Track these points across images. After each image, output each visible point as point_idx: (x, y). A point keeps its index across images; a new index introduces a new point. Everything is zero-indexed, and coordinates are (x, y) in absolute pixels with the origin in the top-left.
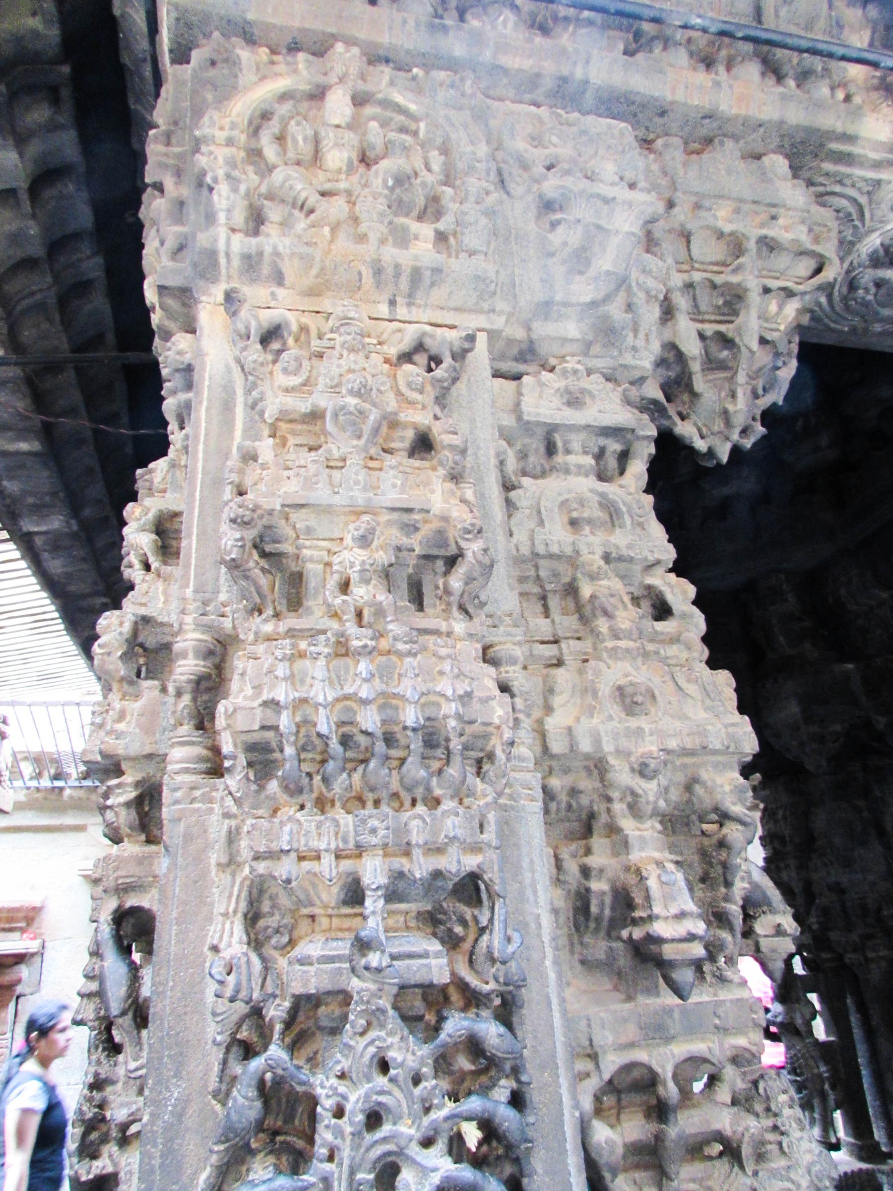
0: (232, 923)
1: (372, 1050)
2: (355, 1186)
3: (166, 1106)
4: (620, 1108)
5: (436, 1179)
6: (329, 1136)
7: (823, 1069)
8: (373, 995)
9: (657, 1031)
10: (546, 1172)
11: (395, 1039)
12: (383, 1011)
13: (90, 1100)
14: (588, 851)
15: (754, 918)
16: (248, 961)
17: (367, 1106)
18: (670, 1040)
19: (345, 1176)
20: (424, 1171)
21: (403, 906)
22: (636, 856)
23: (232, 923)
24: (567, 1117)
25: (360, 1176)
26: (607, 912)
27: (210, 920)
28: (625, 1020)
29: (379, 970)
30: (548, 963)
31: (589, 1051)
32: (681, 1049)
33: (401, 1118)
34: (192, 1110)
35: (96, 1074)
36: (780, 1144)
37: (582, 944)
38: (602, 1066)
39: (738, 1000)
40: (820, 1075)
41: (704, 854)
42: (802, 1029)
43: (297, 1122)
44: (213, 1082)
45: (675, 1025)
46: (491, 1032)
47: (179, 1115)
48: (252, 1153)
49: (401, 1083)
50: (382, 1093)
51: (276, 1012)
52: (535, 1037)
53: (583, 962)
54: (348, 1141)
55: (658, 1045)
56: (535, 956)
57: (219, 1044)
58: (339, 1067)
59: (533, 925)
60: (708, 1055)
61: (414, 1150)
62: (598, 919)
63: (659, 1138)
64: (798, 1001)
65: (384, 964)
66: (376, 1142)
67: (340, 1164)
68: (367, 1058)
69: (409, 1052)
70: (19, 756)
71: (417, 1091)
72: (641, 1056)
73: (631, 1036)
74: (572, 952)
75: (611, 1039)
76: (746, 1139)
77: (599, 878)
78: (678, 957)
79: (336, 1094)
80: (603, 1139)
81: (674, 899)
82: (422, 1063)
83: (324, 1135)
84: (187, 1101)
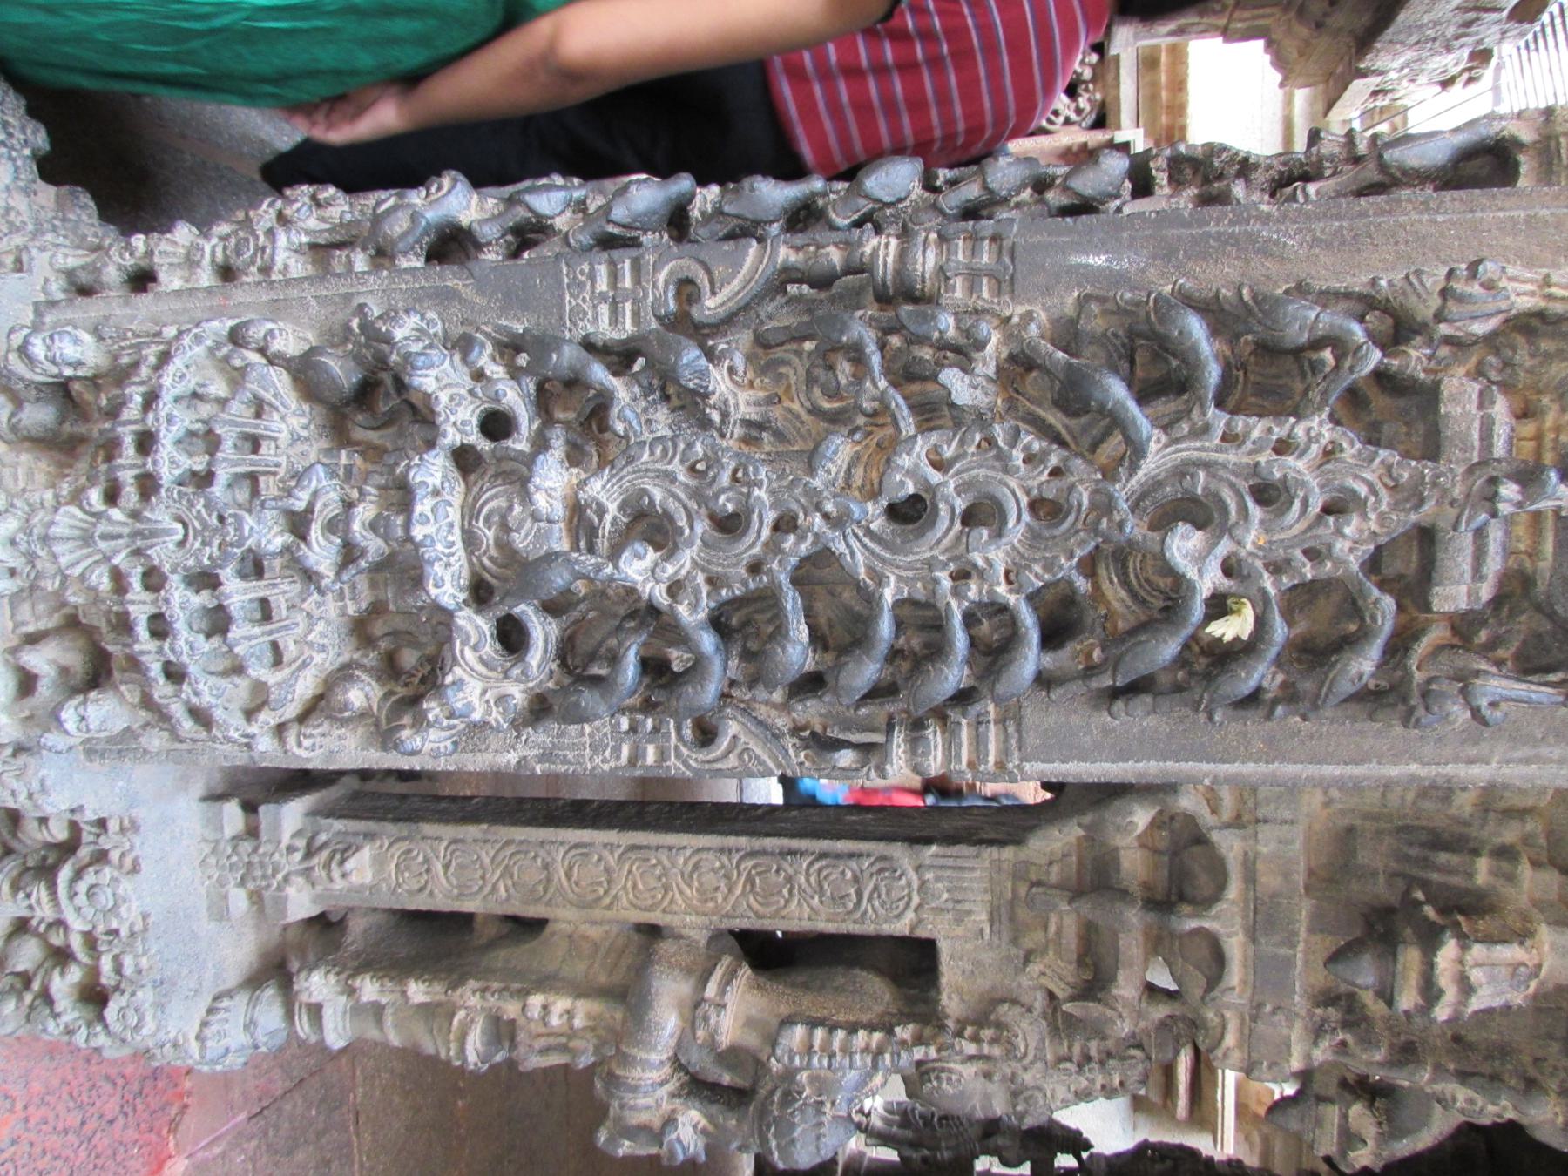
0: (1533, 294)
1: (1363, 490)
2: (1192, 470)
3: (1277, 232)
4: (1156, 852)
5: (1191, 573)
6: (1255, 434)
7: (947, 1154)
8: (1445, 492)
9: (1264, 919)
10: (1143, 731)
11: (1374, 526)
12: (1417, 507)
13: (1231, 161)
14: (1536, 864)
15: (1371, 1106)
16: (1489, 316)
17: (1290, 483)
18: (1252, 935)
19: (1204, 455)
20: (1200, 559)
21: (1549, 547)
22: (1545, 933)
23: (1533, 294)
24: (1205, 767)
25: (1202, 474)
26: (1435, 876)
27: (1530, 263)
28: (1286, 875)
29: (1492, 498)
30: (1414, 767)
31: (1246, 818)
32: (1235, 947)
33: (1267, 531)
34: (1272, 266)
35: (1256, 166)
36: (1070, 1060)
37: (1379, 832)
38: (1226, 832)
39: (1289, 1047)
40: (938, 1148)
41: (1503, 1051)
42: (991, 1142)
43: (1252, 400)
44: (1317, 286)
45: (1269, 946)
46: (1364, 664)
47: (1265, 252)
48: (1233, 340)
49: (1315, 532)
50: (1305, 504)
51: (1415, 359)
52: (1311, 737)
53: (1350, 830)
54: (1245, 460)
55: (1245, 917)
56: (1428, 750)
57: (1374, 282)
58: (1345, 445)
59: (1472, 751)
60: (1222, 985)
61: (1224, 547)
62: (1426, 863)
63: (1124, 894)
64: (1024, 1147)
65: (1501, 506)
66: (1242, 497)
67: (1219, 450)
68: (1352, 483)
69: (1350, 543)
70: (1398, 120)
71: (1298, 553)
72: (1233, 891)
73: (1264, 879)
74: (1375, 817)
75: (1265, 850)
76: (1109, 1013)
77: (1494, 873)
78: (1400, 967)
79: (1310, 440)
80: (1135, 819)
81: (1492, 980)
82: (1338, 562)
83: (1258, 428)
84: (1282, 259)
